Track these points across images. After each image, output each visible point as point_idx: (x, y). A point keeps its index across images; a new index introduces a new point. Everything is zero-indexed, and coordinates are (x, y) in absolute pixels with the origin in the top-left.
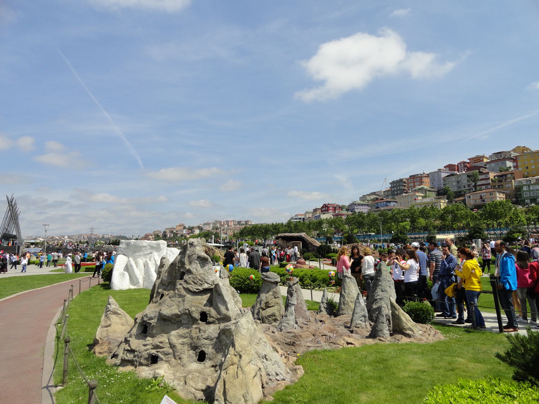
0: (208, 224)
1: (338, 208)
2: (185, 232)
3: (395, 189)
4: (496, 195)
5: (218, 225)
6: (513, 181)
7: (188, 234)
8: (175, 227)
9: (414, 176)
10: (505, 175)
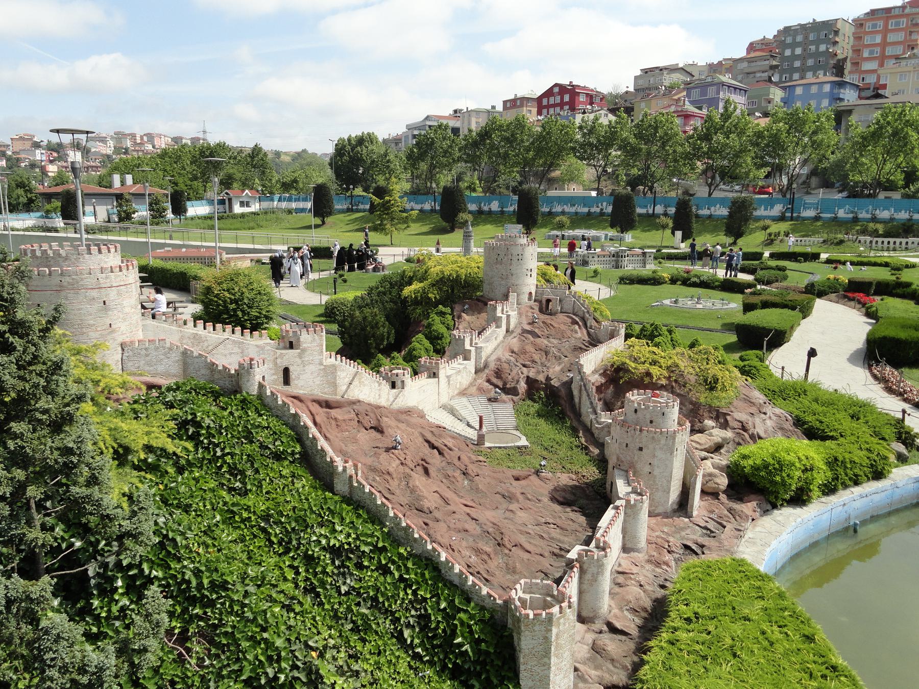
0: (103, 140)
1: (598, 100)
2: (39, 155)
3: (798, 51)
5: (129, 144)
7: (51, 162)
8: (9, 142)
9: (888, 10)
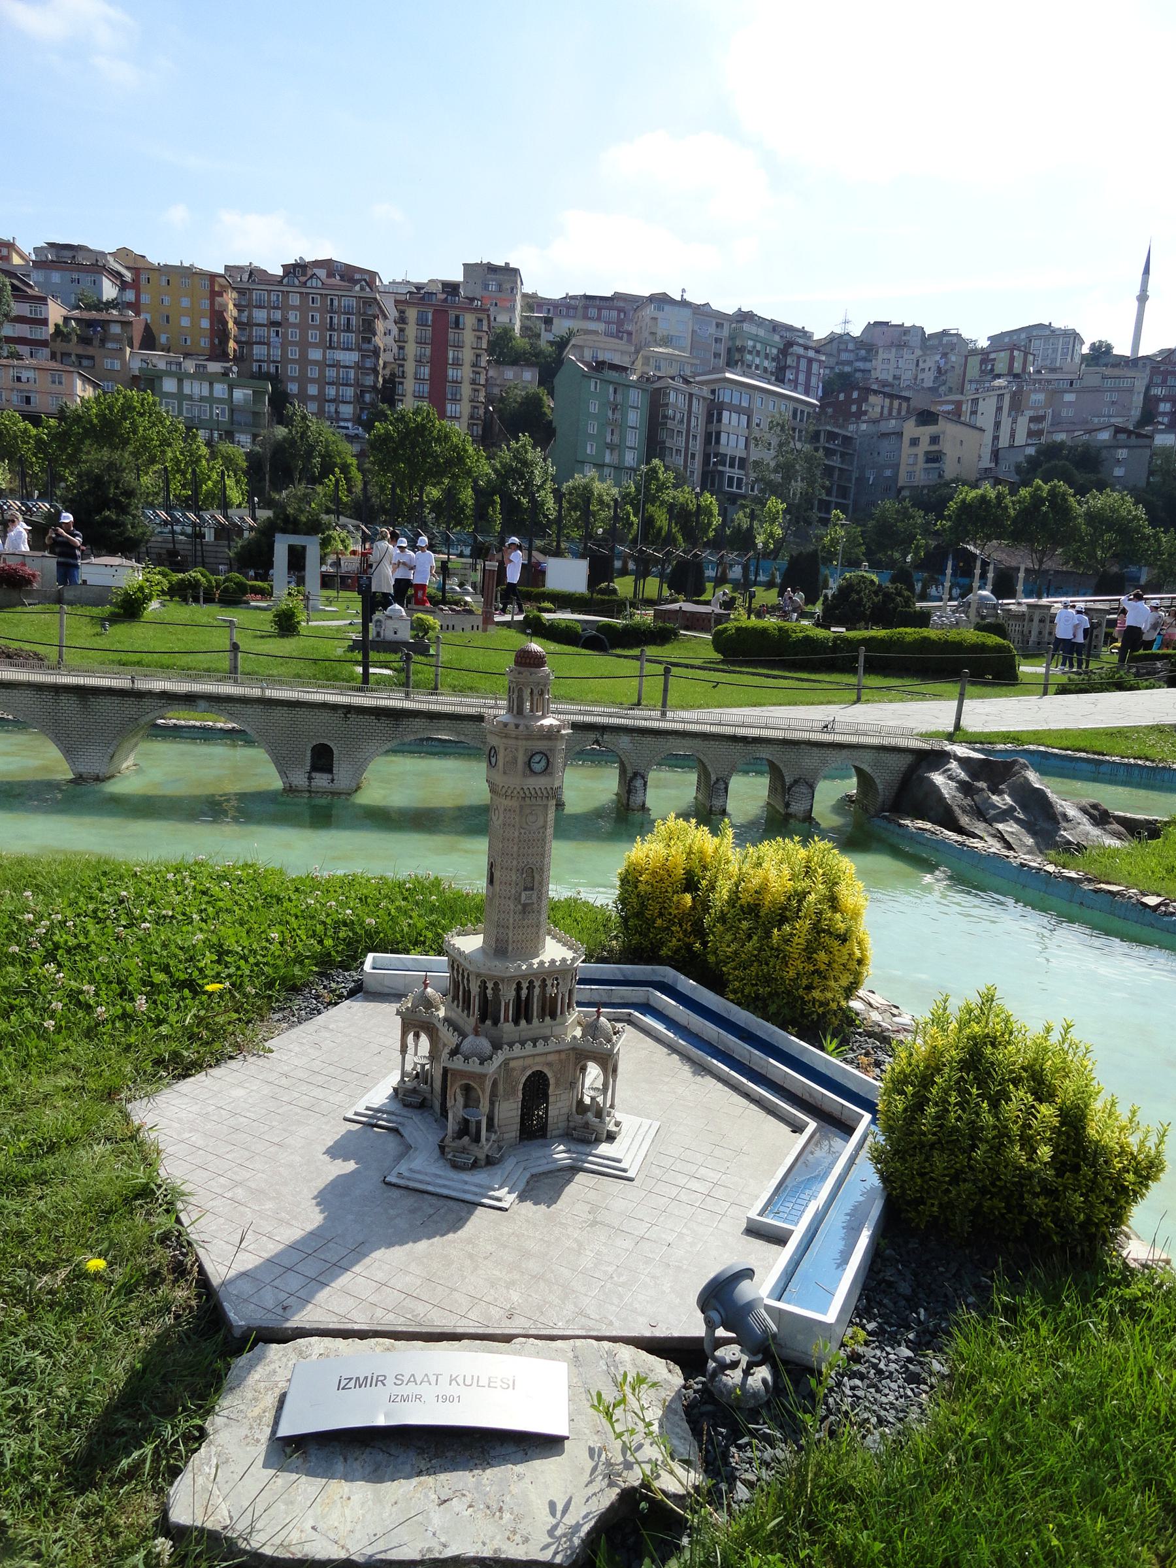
4: (73, 386)
6: (128, 350)
10: (105, 323)
